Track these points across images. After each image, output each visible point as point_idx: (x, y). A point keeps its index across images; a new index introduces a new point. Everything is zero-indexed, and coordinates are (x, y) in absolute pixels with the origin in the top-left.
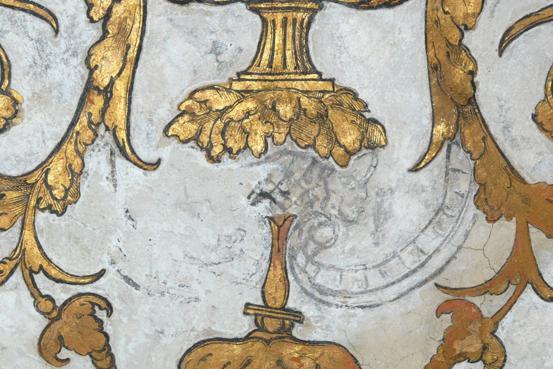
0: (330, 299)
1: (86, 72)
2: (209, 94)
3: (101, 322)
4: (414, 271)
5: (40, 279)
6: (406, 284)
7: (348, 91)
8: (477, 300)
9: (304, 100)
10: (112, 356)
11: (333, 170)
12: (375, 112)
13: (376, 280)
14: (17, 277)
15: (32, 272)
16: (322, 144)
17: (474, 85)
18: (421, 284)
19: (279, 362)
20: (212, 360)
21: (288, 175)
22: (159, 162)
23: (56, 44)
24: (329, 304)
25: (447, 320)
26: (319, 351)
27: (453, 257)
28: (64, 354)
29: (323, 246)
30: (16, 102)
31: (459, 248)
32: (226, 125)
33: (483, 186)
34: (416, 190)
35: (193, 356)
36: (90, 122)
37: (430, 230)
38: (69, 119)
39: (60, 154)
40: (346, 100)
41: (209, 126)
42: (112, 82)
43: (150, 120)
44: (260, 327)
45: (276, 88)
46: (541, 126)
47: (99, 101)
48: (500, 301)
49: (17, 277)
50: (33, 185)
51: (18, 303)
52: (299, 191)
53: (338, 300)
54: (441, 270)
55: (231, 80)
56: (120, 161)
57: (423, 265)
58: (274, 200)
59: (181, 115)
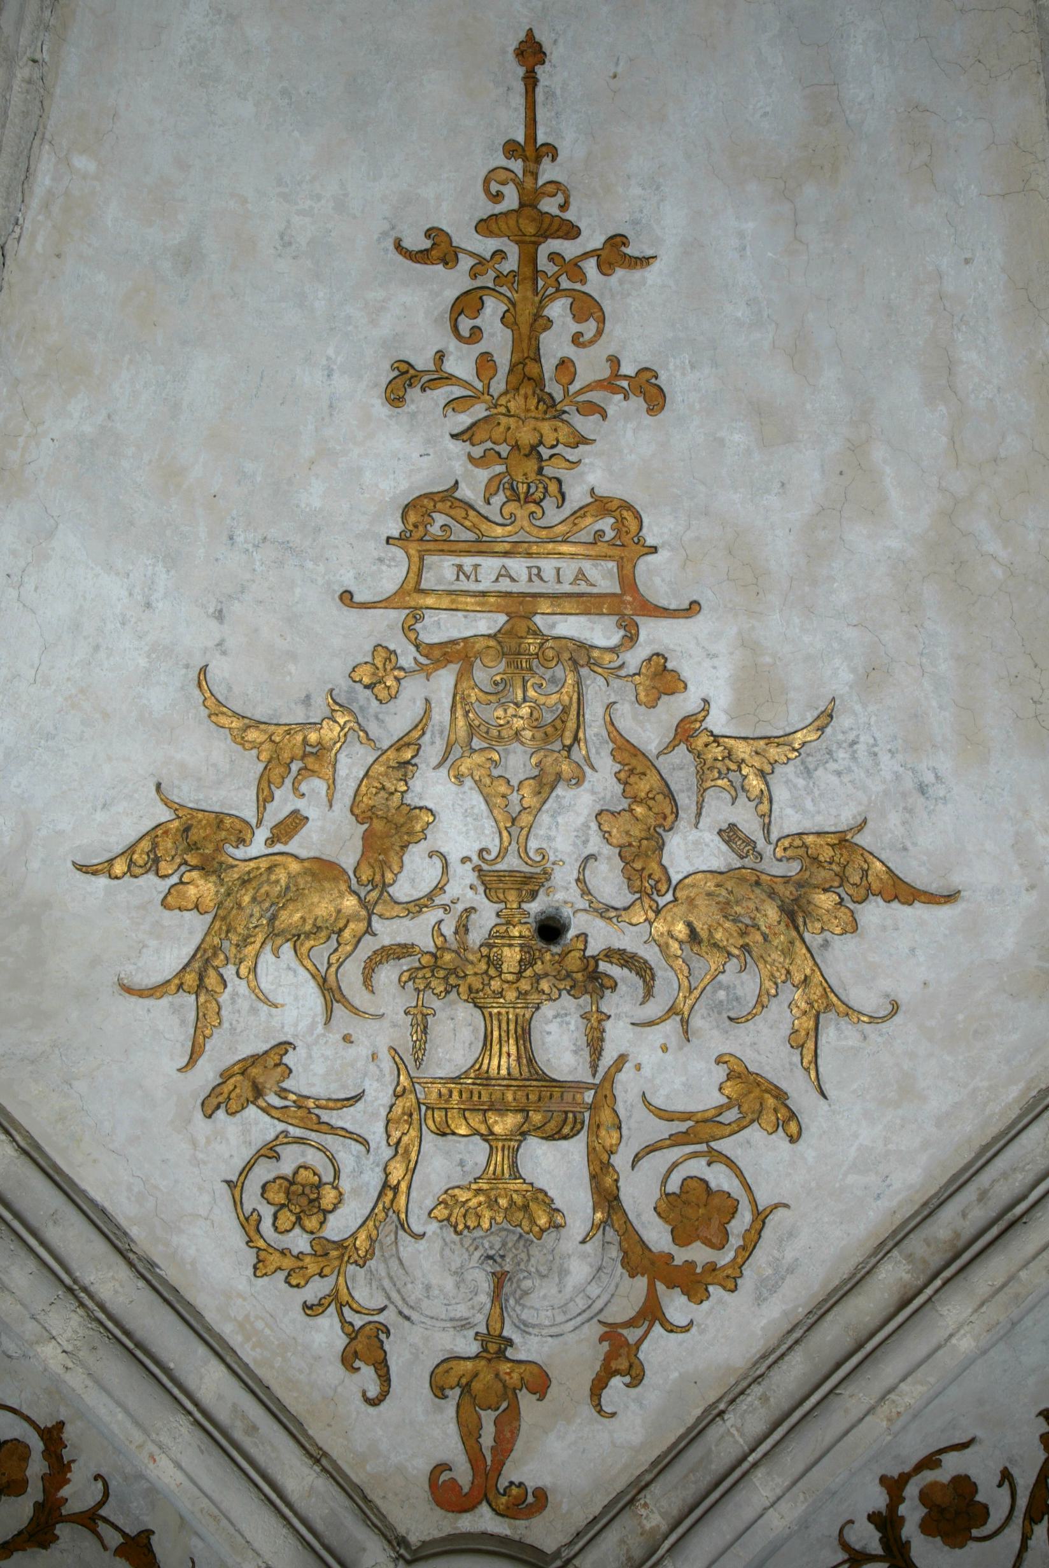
0: (530, 1330)
1: (383, 1176)
2: (456, 1191)
3: (382, 1342)
4: (584, 1311)
5: (346, 1310)
6: (579, 1320)
7: (541, 1191)
8: (625, 1332)
9: (515, 1196)
10: (388, 1367)
11: (532, 1242)
12: (558, 1204)
13: (560, 1318)
14: (332, 1308)
15: (341, 1305)
16: (526, 1224)
17: (618, 1188)
18: (589, 1320)
19: (497, 1375)
20: (452, 1373)
21: (504, 1244)
22: (424, 1234)
23: (368, 1159)
24: (530, 1334)
25: (606, 1346)
26: (523, 1367)
27: (609, 1301)
28: (357, 1364)
29: (526, 1293)
30: (341, 1194)
31: (613, 1295)
32: (467, 1211)
33: (626, 1253)
34: (584, 1256)
35: (440, 1369)
36: (384, 1207)
37: (593, 1283)
38: (371, 1205)
39: (365, 1227)
40: (541, 1196)
41: (456, 1211)
42: (399, 1182)
43: (421, 1208)
44: (485, 1350)
45: (498, 1188)
46: (659, 1214)
47: (390, 1194)
48: (639, 1332)
49: (332, 1308)
50: (346, 1247)
51: (332, 1326)
52: (511, 1255)
53: (536, 1331)
54: (601, 1310)
55: (470, 1183)
56: (401, 1232)
57: (589, 1307)
58: (495, 1261)
59: (440, 1204)
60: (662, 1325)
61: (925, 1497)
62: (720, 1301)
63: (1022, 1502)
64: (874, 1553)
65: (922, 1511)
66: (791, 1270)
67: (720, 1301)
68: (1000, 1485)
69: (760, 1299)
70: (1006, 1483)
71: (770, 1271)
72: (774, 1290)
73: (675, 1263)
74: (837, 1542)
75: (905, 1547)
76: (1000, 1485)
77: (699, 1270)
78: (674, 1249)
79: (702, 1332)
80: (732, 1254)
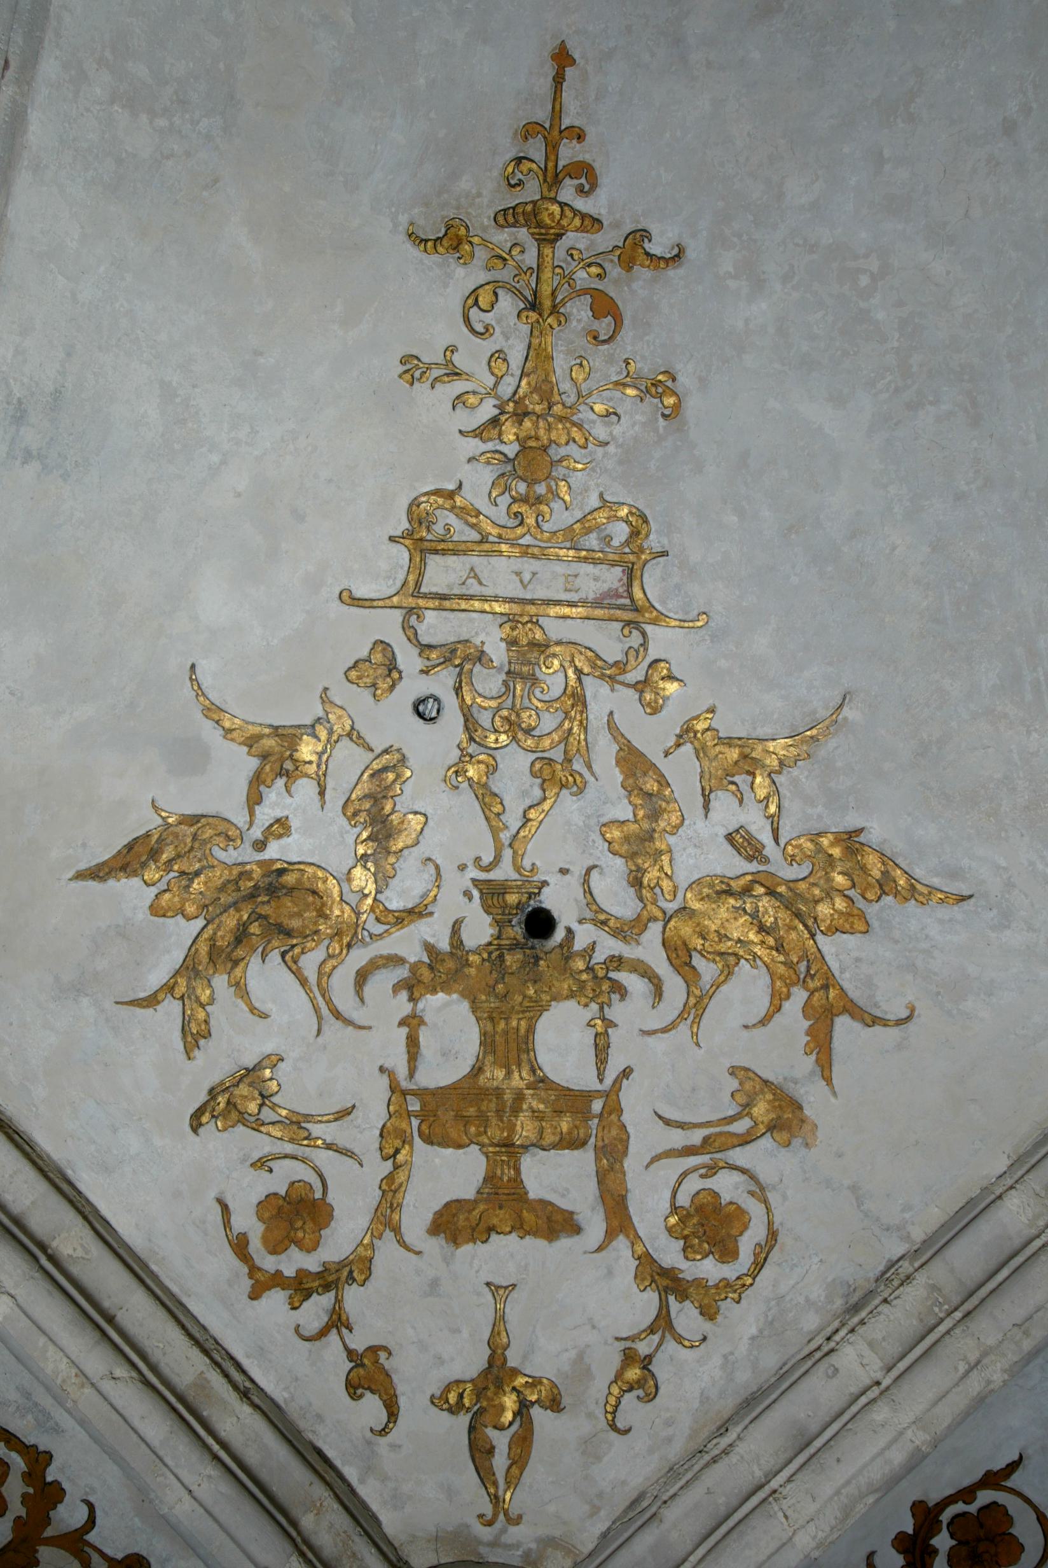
60: (87, 1533)
61: (275, 1248)
62: (62, 1470)
63: (289, 1148)
64: (333, 1301)
65: (294, 1251)
66: (27, 1395)
67: (62, 1470)
68: (271, 1171)
69: (57, 1430)
70: (270, 1164)
71: (30, 1417)
72: (48, 1416)
73: (24, 1515)
74: (317, 1343)
75: (326, 1268)
76: (271, 1171)
77: (31, 1490)
78: (10, 1516)
79: (93, 1490)
80: (14, 1455)
